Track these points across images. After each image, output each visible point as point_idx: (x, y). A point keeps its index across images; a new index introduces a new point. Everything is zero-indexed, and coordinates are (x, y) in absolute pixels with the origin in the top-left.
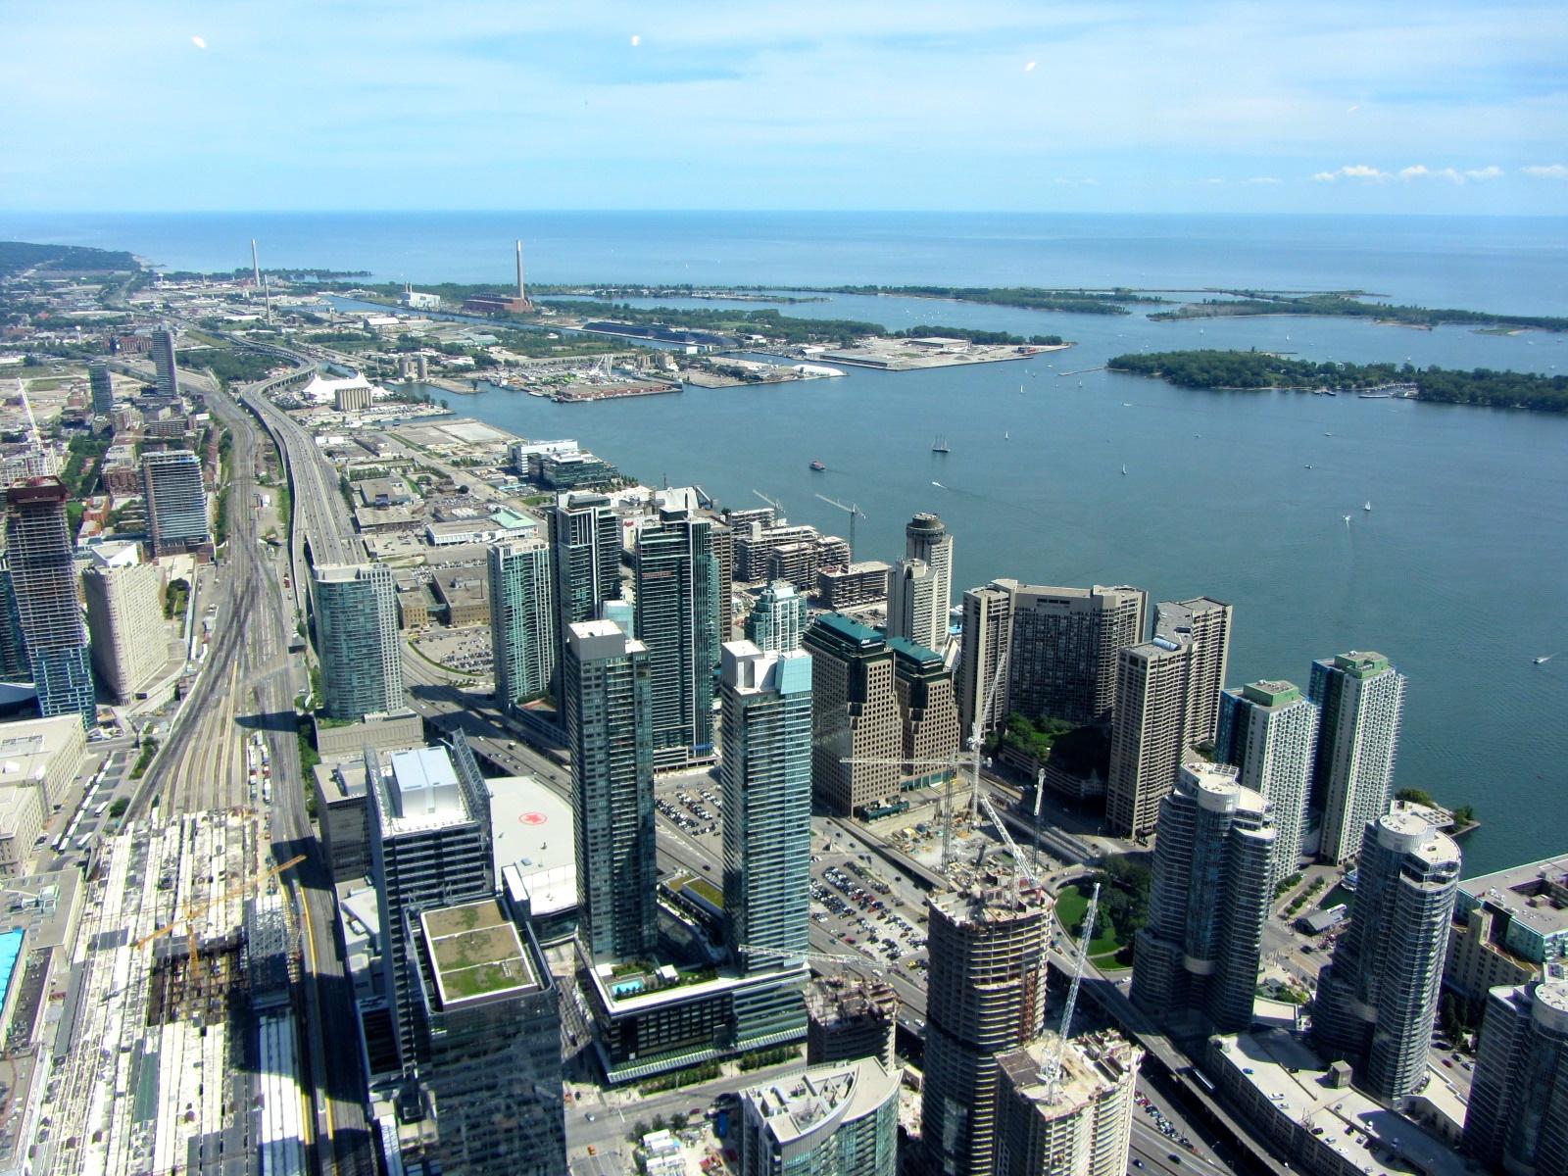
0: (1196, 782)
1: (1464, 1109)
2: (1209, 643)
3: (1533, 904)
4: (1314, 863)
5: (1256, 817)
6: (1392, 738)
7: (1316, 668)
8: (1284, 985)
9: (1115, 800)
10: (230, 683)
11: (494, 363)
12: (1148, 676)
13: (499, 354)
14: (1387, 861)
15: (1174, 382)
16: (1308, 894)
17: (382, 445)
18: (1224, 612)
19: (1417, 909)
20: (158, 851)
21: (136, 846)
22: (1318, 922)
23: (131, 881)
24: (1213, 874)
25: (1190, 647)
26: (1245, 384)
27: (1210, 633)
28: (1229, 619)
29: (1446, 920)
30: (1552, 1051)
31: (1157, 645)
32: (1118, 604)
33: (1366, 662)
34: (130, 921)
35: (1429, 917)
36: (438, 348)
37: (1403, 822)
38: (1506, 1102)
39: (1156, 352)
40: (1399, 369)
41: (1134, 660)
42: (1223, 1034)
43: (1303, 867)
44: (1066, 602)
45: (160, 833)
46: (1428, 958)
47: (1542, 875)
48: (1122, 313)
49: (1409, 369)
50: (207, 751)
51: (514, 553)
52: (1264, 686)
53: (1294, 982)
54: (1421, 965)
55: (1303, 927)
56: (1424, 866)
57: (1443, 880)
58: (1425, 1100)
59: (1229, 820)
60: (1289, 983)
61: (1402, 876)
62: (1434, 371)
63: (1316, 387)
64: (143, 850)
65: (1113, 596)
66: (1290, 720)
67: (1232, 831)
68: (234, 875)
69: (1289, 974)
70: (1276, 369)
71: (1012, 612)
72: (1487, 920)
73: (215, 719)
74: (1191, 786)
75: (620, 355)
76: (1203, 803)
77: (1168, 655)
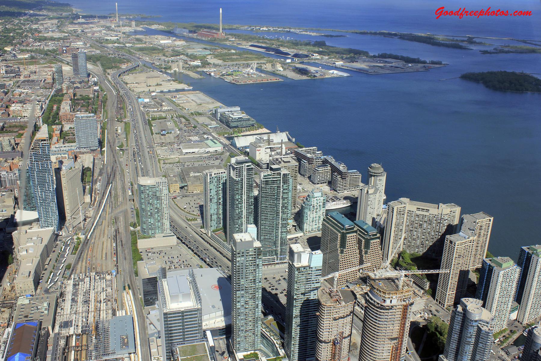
10: (106, 214)
11: (209, 64)
13: (211, 60)
17: (164, 103)
20: (83, 287)
21: (75, 285)
23: (73, 300)
26: (517, 90)
34: (74, 317)
36: (187, 55)
39: (481, 72)
41: (451, 242)
45: (83, 280)
50: (98, 244)
51: (213, 175)
64: (77, 287)
68: (109, 300)
71: (406, 212)
73: (101, 231)
75: (259, 62)
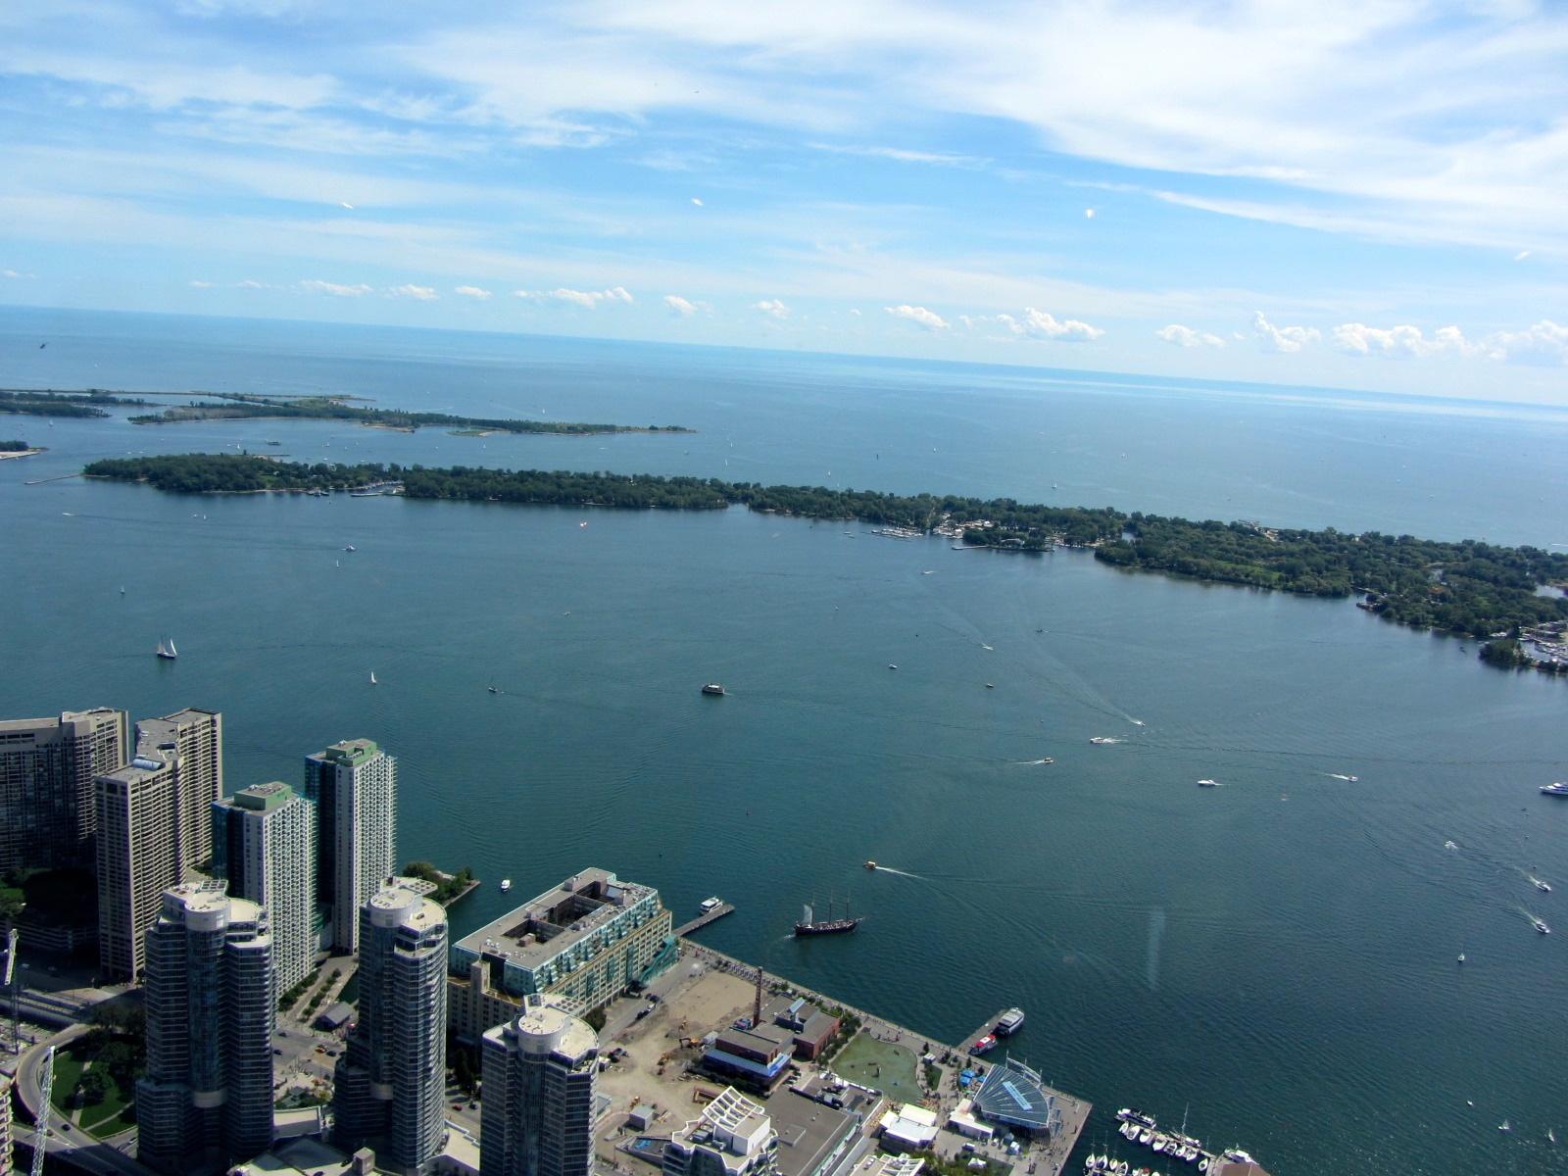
0: (182, 905)
1: (478, 1151)
2: (200, 756)
3: (522, 944)
4: (332, 956)
5: (249, 926)
6: (390, 818)
7: (310, 763)
8: (307, 1090)
9: (109, 944)
12: (130, 802)
14: (388, 936)
15: (161, 487)
16: (325, 989)
18: (213, 722)
19: (413, 978)
22: (336, 1017)
24: (212, 997)
25: (175, 763)
26: (238, 487)
27: (200, 745)
28: (219, 728)
29: (440, 981)
30: (538, 1074)
31: (138, 766)
32: (93, 729)
33: (356, 750)
35: (424, 982)
37: (392, 897)
38: (510, 1133)
40: (386, 468)
41: (113, 787)
42: (242, 1164)
43: (319, 964)
44: (29, 735)
46: (429, 1022)
47: (528, 916)
48: (98, 415)
49: (395, 468)
52: (254, 791)
53: (317, 1084)
54: (425, 1030)
55: (324, 1025)
56: (414, 935)
57: (433, 944)
58: (447, 1158)
59: (222, 937)
60: (312, 1086)
61: (396, 950)
62: (418, 469)
63: (309, 488)
65: (85, 721)
66: (286, 819)
67: (227, 948)
69: (312, 1077)
70: (270, 472)
72: (486, 970)
74: (176, 909)
76: (192, 926)
77: (151, 775)
